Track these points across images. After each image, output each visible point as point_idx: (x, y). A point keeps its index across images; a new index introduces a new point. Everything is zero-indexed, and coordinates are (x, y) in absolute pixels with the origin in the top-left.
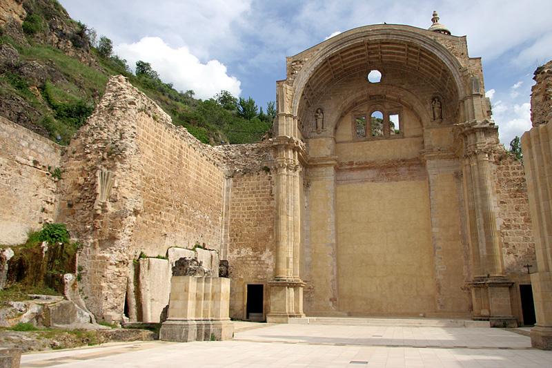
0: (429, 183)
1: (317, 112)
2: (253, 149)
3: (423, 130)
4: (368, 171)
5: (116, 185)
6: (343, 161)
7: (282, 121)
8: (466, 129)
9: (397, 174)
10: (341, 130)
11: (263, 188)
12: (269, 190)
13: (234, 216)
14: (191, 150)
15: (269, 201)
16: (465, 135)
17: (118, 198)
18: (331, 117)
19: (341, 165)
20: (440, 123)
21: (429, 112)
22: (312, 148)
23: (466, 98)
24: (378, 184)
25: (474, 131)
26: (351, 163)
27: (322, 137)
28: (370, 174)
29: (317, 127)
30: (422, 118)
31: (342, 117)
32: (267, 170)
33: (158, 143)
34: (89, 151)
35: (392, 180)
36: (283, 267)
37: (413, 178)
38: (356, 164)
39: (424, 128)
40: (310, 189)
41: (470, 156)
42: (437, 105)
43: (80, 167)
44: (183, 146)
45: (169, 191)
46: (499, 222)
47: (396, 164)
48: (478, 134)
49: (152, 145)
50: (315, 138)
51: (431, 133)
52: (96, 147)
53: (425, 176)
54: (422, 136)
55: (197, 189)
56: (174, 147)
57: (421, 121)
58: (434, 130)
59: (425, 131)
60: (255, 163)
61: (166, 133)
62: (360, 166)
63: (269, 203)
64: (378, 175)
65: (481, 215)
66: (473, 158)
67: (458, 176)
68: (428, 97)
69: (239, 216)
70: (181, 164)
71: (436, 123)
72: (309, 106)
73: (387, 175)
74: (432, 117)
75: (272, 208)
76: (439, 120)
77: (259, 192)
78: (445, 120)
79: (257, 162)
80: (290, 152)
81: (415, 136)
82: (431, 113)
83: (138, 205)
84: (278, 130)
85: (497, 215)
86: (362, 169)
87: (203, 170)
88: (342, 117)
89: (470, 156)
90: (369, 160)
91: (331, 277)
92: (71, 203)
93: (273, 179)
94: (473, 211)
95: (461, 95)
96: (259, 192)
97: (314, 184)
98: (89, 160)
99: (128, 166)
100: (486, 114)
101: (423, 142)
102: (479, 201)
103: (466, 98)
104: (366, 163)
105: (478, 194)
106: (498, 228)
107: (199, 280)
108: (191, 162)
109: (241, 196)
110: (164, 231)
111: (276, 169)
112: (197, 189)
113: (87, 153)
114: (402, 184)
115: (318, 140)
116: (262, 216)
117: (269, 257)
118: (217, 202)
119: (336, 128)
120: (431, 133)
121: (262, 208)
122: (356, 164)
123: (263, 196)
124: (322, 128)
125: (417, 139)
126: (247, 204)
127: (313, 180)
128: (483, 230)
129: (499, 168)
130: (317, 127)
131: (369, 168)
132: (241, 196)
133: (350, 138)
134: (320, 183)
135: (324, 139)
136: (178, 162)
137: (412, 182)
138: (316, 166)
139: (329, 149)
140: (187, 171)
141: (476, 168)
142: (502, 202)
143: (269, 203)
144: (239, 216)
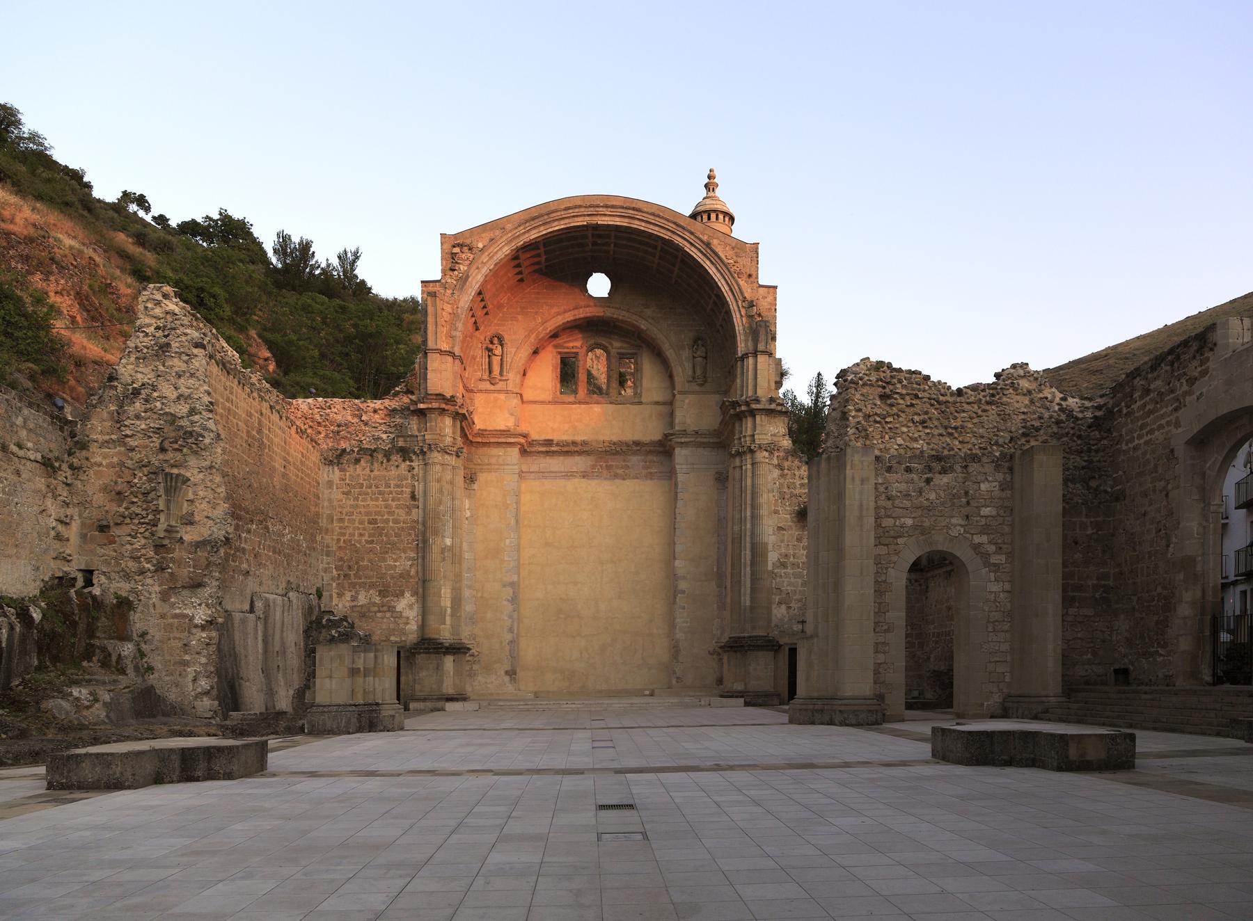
0: (676, 485)
1: (492, 342)
2: (375, 411)
3: (674, 395)
4: (577, 459)
5: (191, 496)
6: (534, 436)
7: (434, 362)
8: (743, 408)
9: (627, 467)
10: (531, 378)
11: (398, 486)
12: (408, 490)
13: (344, 534)
14: (275, 417)
15: (409, 510)
16: (740, 417)
17: (197, 518)
18: (517, 353)
19: (531, 444)
22: (480, 410)
23: (745, 356)
24: (594, 482)
25: (752, 413)
26: (549, 442)
27: (499, 391)
28: (579, 463)
29: (490, 372)
30: (675, 373)
31: (536, 352)
32: (405, 453)
33: (229, 410)
34: (129, 432)
35: (616, 476)
36: (432, 621)
37: (650, 476)
38: (558, 445)
40: (475, 486)
41: (744, 452)
43: (115, 460)
44: (264, 411)
45: (248, 496)
46: (773, 557)
47: (624, 448)
48: (758, 417)
49: (222, 416)
50: (487, 391)
52: (143, 426)
53: (671, 474)
54: (671, 403)
55: (286, 489)
56: (250, 415)
57: (671, 377)
58: (692, 397)
59: (678, 396)
60: (379, 438)
61: (240, 391)
62: (565, 449)
63: (408, 513)
64: (593, 467)
65: (748, 545)
66: (749, 456)
67: (722, 479)
69: (352, 535)
70: (262, 446)
72: (477, 329)
73: (608, 467)
74: (690, 373)
75: (414, 521)
77: (391, 493)
79: (384, 436)
80: (448, 421)
81: (657, 403)
82: (688, 366)
83: (231, 530)
84: (426, 379)
85: (770, 547)
86: (567, 453)
87: (292, 451)
88: (536, 352)
89: (744, 452)
90: (579, 438)
91: (509, 637)
92: (105, 523)
93: (415, 472)
94: (738, 540)
95: (741, 348)
96: (391, 493)
97: (482, 477)
98: (132, 450)
99: (208, 463)
100: (773, 385)
101: (672, 414)
102: (749, 526)
103: (745, 356)
104: (574, 443)
105: (749, 514)
106: (770, 568)
107: (355, 650)
108: (276, 440)
109: (356, 499)
110: (245, 566)
111: (423, 453)
112: (286, 489)
113: (127, 436)
114: (631, 485)
115: (493, 396)
116: (397, 535)
117: (411, 607)
118: (313, 509)
119: (524, 375)
121: (396, 521)
122: (558, 445)
123: (399, 500)
124: (501, 374)
125: (659, 408)
126: (368, 514)
127: (481, 471)
128: (748, 569)
129: (782, 476)
130: (490, 372)
131: (580, 453)
132: (356, 499)
133: (546, 395)
134: (493, 476)
135: (502, 396)
136: (257, 444)
137: (649, 482)
138: (488, 444)
139: (512, 414)
140: (271, 458)
141: (749, 474)
142: (780, 528)
143: (408, 513)
144: (352, 535)
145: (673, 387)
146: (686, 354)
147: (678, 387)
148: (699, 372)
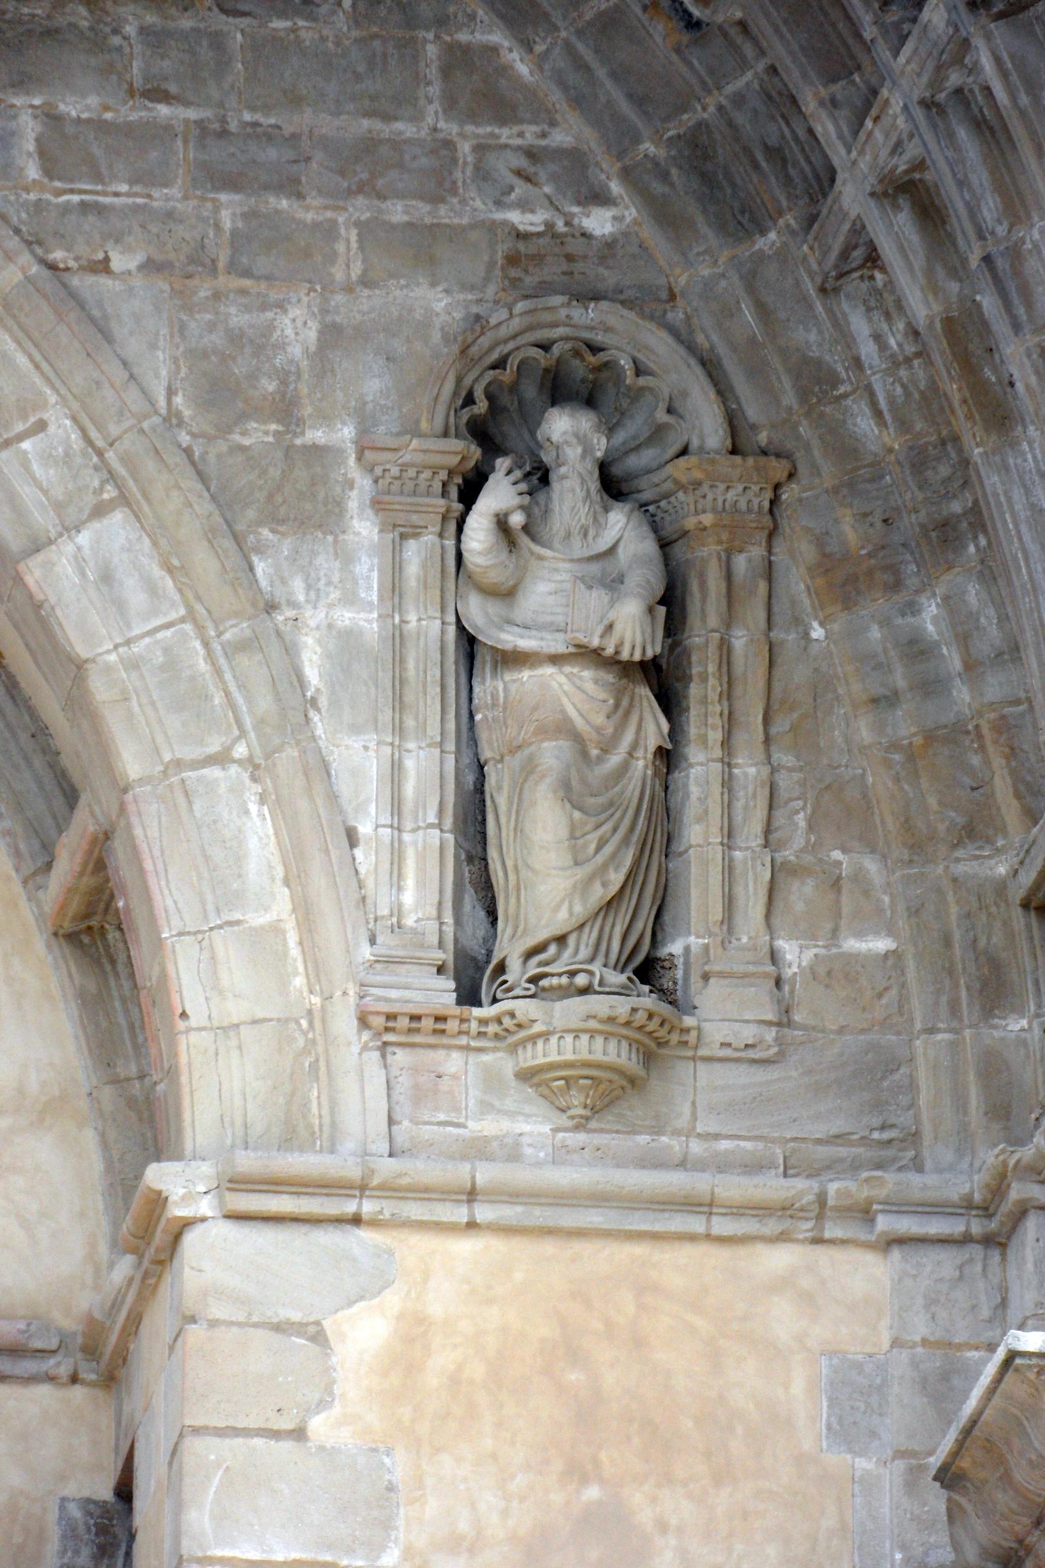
3: (152, 1240)
20: (606, 1095)
21: (358, 758)
30: (170, 897)
39: (183, 1184)
42: (574, 591)
51: (363, 1333)
58: (447, 1273)
59: (217, 1258)
68: (366, 330)
71: (486, 1105)
74: (418, 892)
76: (570, 1030)
78: (724, 1013)
82: (385, 779)
120: (363, 1333)
145: (138, 1114)
146: (352, 592)
147: (219, 1084)
148: (551, 877)
